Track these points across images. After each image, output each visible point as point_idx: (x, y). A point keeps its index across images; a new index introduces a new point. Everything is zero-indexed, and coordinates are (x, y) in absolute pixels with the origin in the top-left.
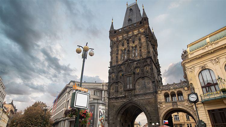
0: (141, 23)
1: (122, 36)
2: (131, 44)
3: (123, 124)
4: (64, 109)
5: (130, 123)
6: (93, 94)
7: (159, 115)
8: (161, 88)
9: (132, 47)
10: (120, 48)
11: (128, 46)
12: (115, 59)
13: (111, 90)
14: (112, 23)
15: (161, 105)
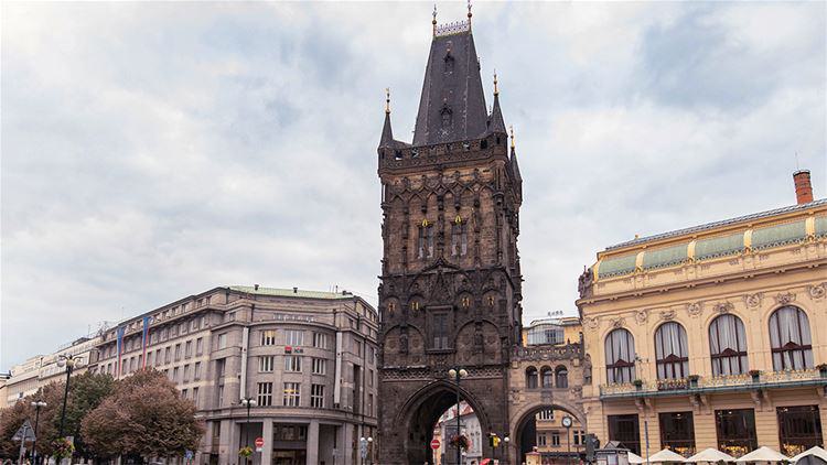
0: (484, 145)
1: (420, 177)
2: (449, 214)
3: (412, 435)
4: (202, 384)
5: (424, 432)
6: (310, 343)
7: (511, 417)
8: (521, 353)
9: (453, 224)
10: (413, 218)
11: (441, 219)
12: (396, 250)
13: (387, 348)
14: (388, 113)
15: (516, 395)
